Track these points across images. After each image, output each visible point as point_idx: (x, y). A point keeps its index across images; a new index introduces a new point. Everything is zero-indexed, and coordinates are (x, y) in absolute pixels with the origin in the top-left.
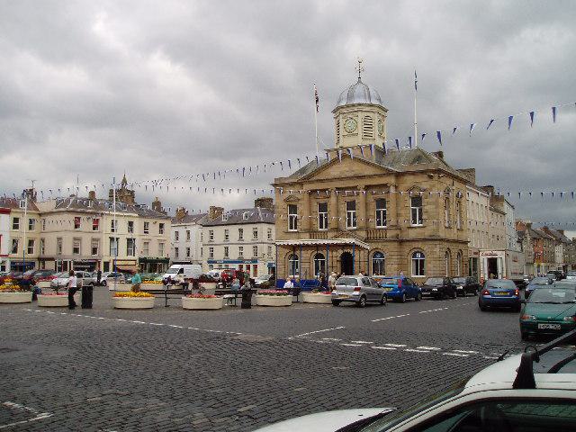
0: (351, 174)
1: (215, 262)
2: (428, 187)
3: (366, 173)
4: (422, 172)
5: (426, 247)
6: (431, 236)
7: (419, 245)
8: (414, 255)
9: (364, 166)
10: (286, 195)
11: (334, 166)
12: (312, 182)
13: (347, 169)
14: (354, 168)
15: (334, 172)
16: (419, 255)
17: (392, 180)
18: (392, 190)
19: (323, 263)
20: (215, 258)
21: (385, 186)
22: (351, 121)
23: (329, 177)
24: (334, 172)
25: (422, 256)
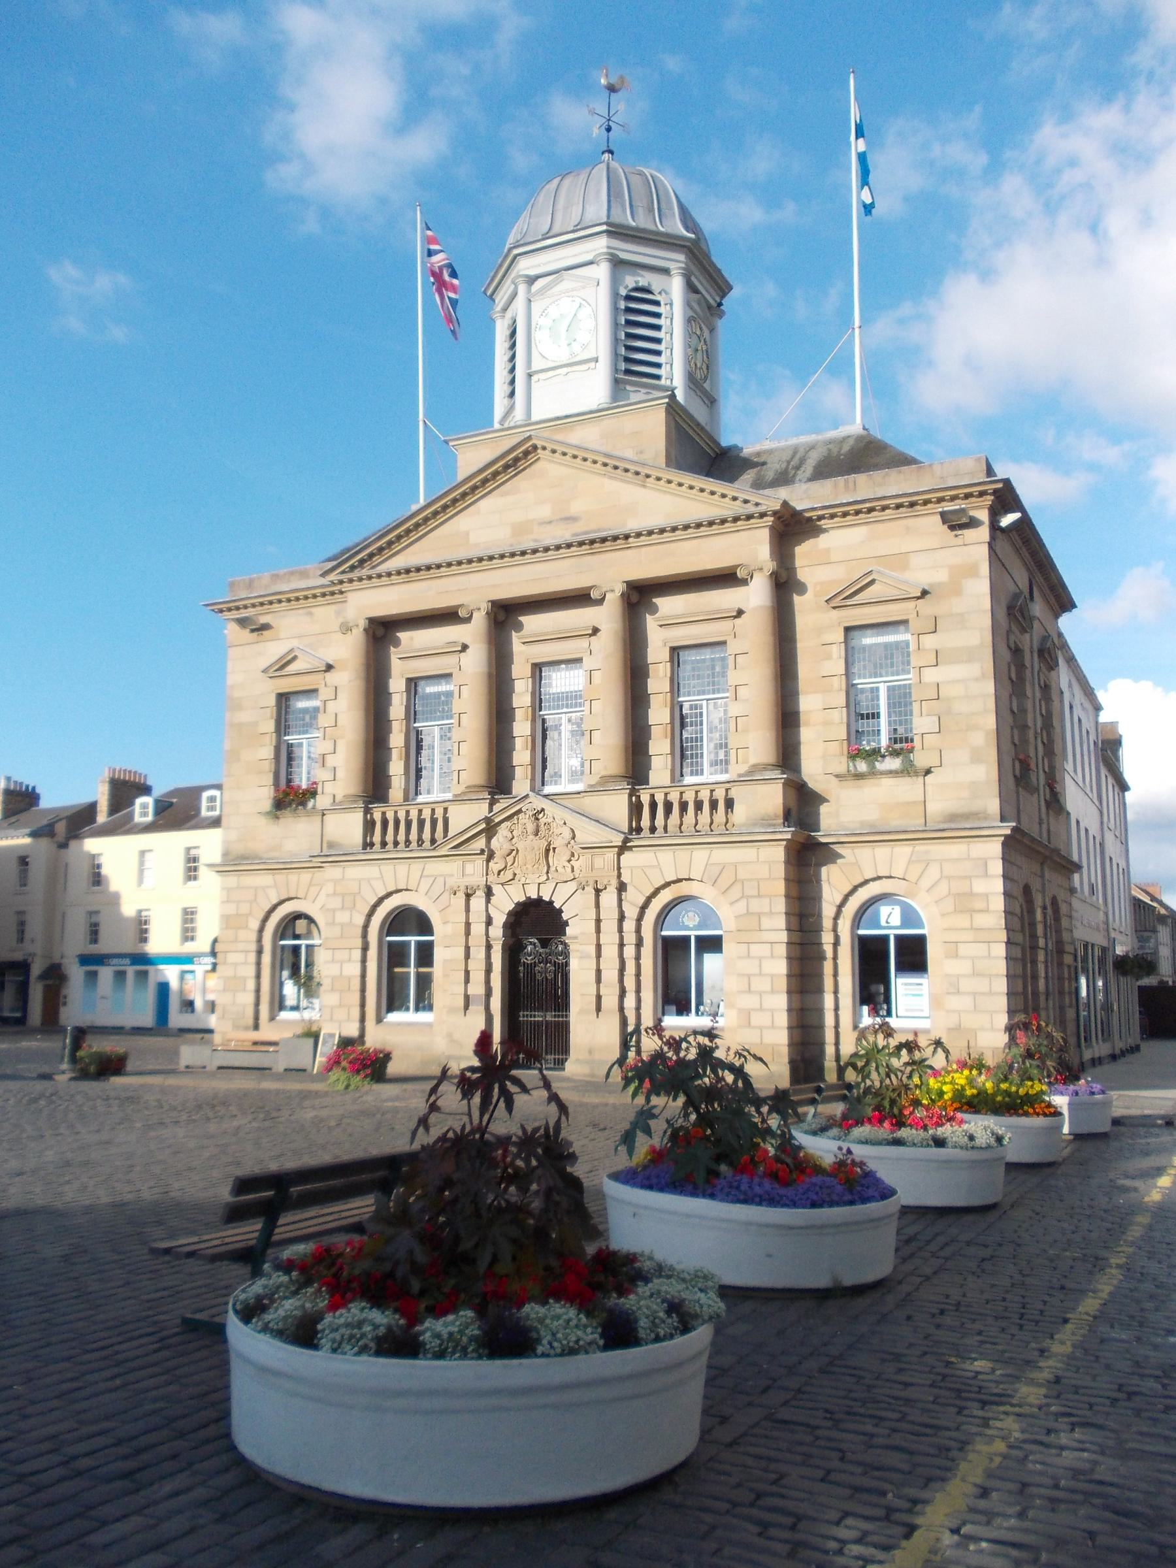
0: (564, 534)
1: (100, 959)
3: (632, 525)
4: (911, 504)
6: (953, 817)
11: (483, 504)
13: (545, 512)
14: (576, 508)
20: (103, 947)
21: (726, 578)
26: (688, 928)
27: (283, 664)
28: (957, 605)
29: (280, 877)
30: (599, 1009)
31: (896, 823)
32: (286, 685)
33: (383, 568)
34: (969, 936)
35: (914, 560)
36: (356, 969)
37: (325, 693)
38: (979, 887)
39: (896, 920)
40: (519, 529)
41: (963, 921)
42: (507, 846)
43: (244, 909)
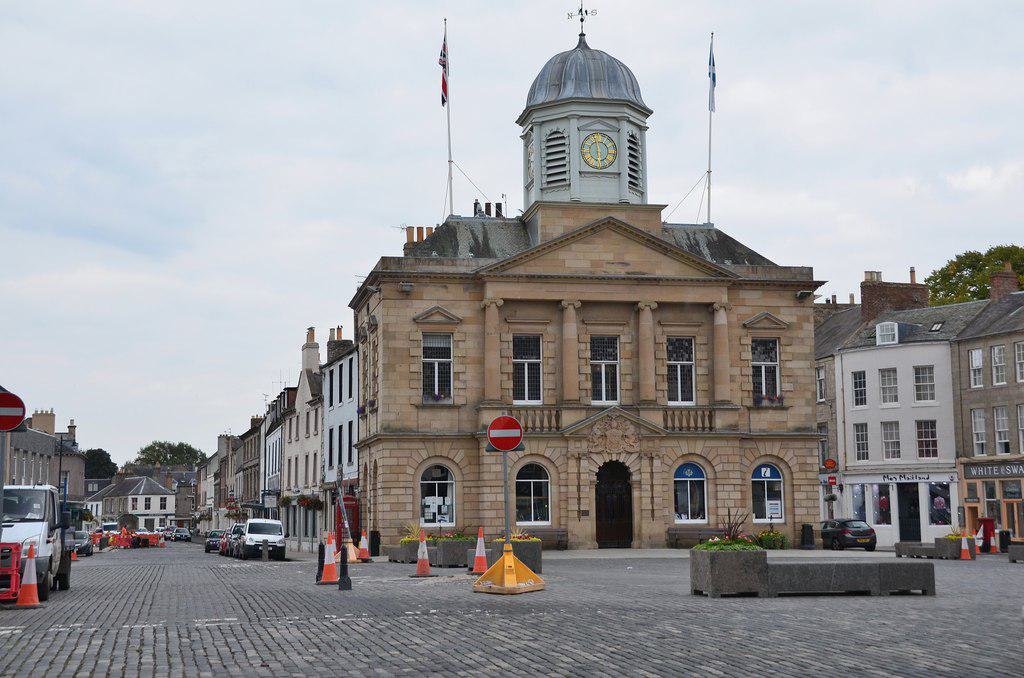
0: (621, 271)
2: (794, 319)
3: (658, 274)
5: (791, 455)
6: (798, 429)
7: (775, 449)
8: (757, 472)
9: (655, 257)
10: (419, 307)
11: (574, 246)
12: (518, 279)
13: (610, 257)
14: (627, 258)
15: (577, 259)
16: (766, 472)
17: (719, 296)
18: (721, 318)
19: (541, 490)
22: (599, 138)
23: (566, 273)
24: (577, 259)
25: (775, 473)
26: (687, 477)
27: (429, 314)
28: (801, 334)
29: (429, 445)
30: (653, 516)
31: (775, 431)
32: (428, 328)
33: (505, 273)
34: (806, 482)
35: (782, 310)
36: (501, 498)
37: (457, 336)
38: (809, 460)
39: (768, 474)
40: (595, 264)
41: (803, 475)
42: (599, 433)
43: (403, 461)
